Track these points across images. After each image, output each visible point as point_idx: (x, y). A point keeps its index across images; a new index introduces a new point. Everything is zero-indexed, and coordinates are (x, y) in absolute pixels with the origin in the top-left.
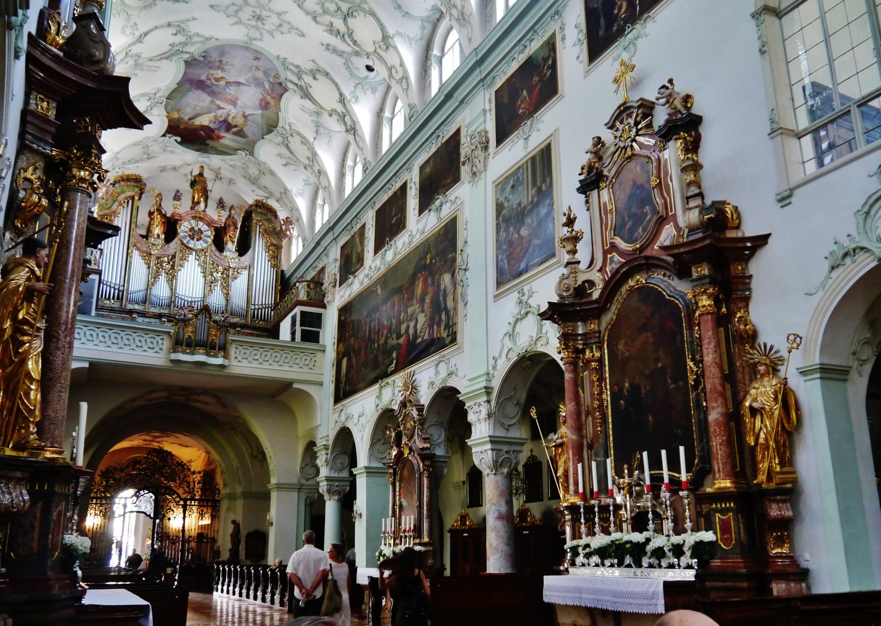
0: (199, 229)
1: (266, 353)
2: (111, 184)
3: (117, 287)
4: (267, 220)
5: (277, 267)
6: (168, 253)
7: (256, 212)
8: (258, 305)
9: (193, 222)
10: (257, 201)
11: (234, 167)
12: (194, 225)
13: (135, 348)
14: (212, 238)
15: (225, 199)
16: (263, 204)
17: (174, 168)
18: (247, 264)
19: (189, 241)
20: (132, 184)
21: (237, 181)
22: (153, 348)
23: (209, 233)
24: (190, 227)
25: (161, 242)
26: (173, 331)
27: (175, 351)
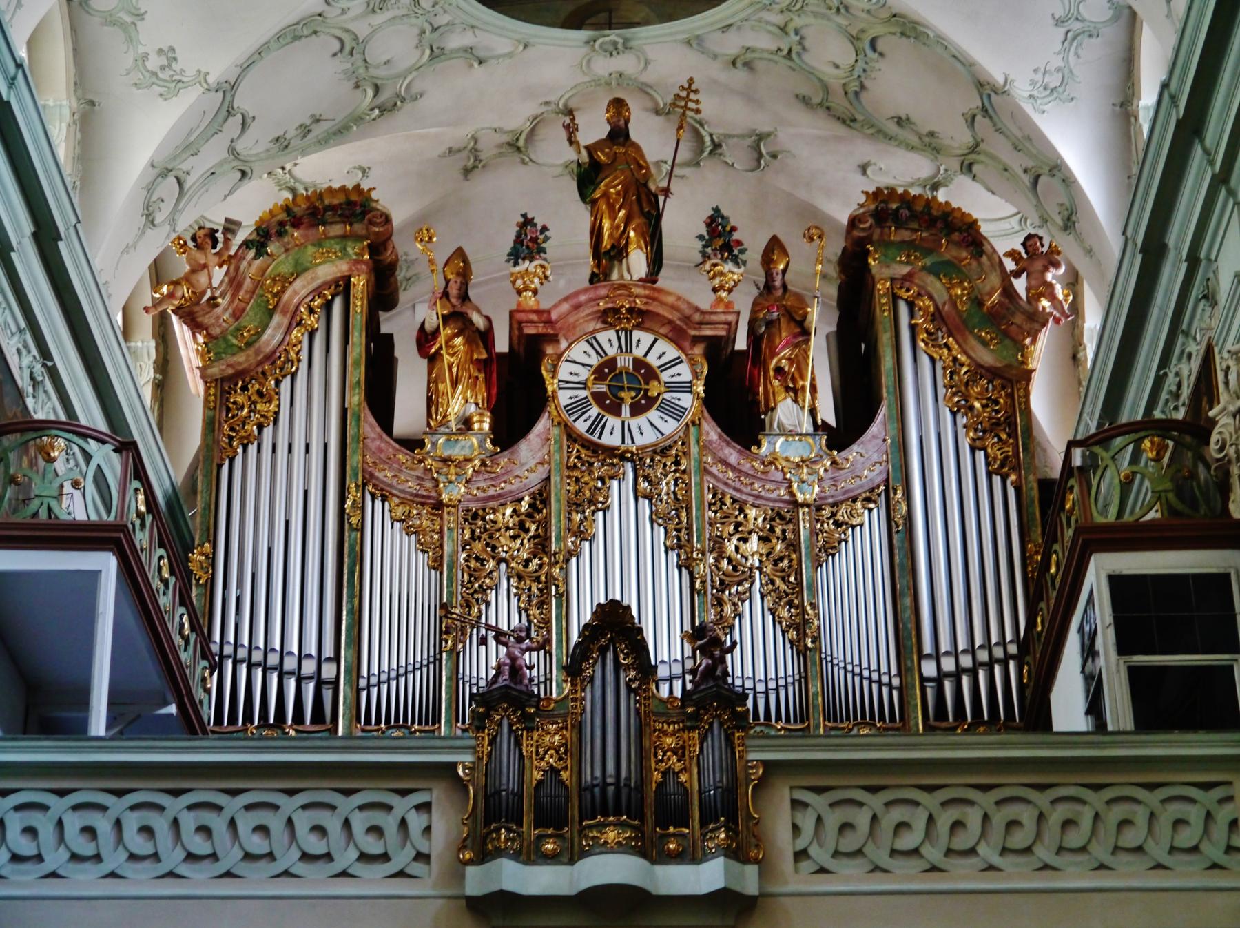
0: (639, 363)
1: (952, 814)
2: (246, 244)
3: (309, 667)
4: (934, 271)
5: (1016, 468)
6: (516, 485)
7: (885, 244)
8: (955, 654)
9: (607, 337)
10: (877, 195)
11: (748, 65)
12: (612, 351)
13: (300, 868)
14: (700, 389)
15: (737, 216)
16: (907, 200)
17: (514, 146)
18: (872, 475)
19: (599, 418)
20: (336, 230)
21: (784, 138)
22: (385, 857)
23: (684, 372)
24: (594, 361)
25: (473, 445)
26: (468, 758)
27: (483, 857)
